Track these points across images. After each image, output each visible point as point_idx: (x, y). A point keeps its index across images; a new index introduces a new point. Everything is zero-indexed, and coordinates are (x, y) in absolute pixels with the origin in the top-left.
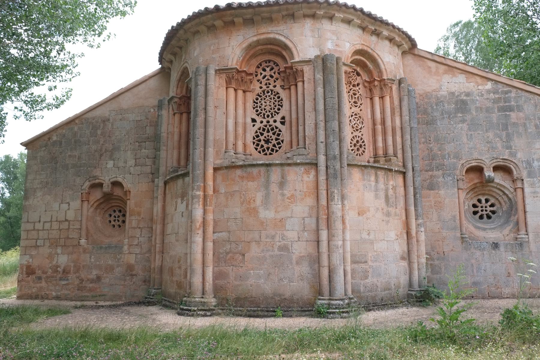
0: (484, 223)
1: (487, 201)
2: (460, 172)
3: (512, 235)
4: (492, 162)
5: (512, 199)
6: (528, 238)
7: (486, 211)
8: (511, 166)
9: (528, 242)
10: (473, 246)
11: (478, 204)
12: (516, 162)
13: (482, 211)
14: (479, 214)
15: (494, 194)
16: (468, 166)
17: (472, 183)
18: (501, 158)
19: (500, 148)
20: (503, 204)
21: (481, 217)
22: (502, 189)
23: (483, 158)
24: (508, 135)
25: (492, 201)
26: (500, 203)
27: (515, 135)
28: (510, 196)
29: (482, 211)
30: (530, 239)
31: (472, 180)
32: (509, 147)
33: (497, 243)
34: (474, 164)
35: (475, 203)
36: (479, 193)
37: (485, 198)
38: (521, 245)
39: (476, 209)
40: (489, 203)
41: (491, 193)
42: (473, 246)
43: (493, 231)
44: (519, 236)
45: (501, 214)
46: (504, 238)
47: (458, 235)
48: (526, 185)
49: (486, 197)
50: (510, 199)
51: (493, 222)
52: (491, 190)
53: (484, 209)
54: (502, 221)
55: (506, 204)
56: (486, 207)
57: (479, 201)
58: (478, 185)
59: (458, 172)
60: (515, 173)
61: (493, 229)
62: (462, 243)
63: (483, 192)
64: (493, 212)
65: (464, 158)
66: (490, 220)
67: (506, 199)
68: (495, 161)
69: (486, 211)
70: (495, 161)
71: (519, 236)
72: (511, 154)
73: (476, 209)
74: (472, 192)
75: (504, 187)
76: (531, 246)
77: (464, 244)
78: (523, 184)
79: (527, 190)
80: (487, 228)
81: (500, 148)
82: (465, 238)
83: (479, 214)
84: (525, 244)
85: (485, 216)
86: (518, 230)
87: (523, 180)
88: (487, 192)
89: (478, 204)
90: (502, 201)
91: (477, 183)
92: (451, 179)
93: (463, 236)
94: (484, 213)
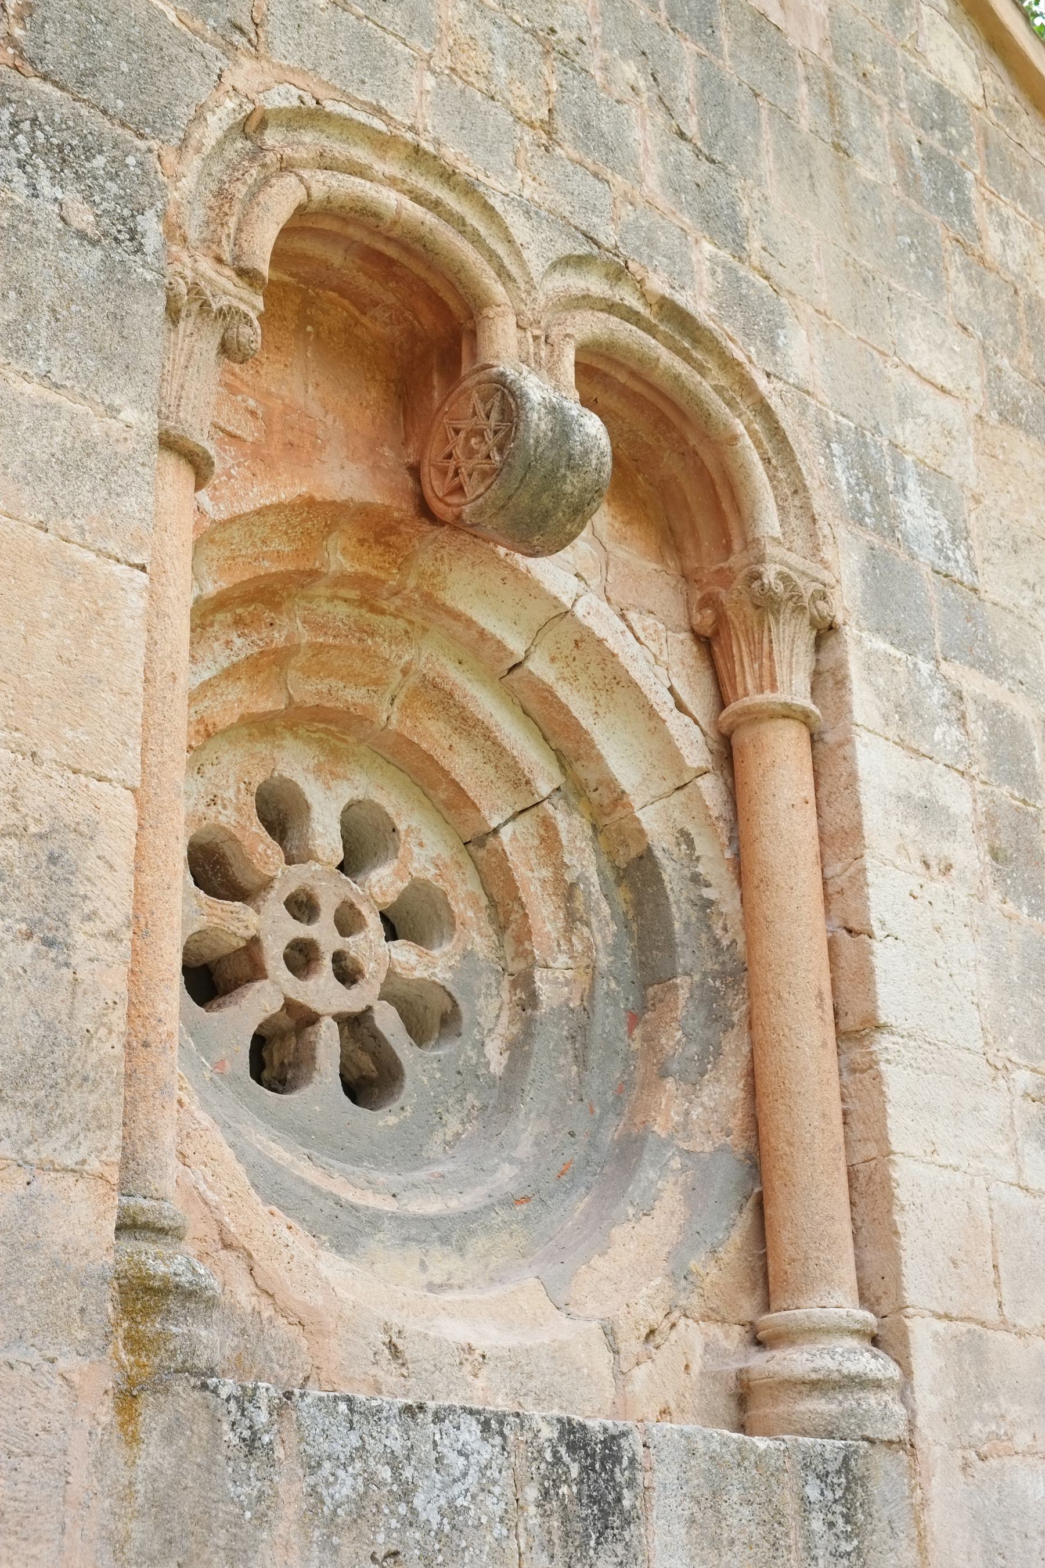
0: (301, 1134)
1: (363, 844)
2: (214, 215)
3: (693, 1335)
4: (578, 282)
5: (671, 873)
6: (905, 1389)
7: (347, 974)
8: (740, 428)
9: (905, 1445)
10: (291, 1488)
11: (262, 851)
12: (774, 402)
13: (301, 957)
14: (257, 1004)
15: (464, 764)
16: (325, 184)
17: (287, 488)
18: (658, 284)
19: (652, 182)
20: (544, 915)
21: (274, 1060)
22: (578, 704)
23: (497, 187)
24: (713, 91)
25: (422, 854)
26: (504, 908)
27: (768, 136)
28: (655, 821)
29: (301, 957)
30: (928, 1401)
31: (286, 441)
32: (725, 225)
33: (612, 1440)
34: (390, 200)
35: (227, 818)
36: (307, 690)
37: (346, 793)
38: (847, 1485)
39: (236, 921)
40: (383, 882)
41: (434, 734)
42: (291, 1488)
43: (443, 1264)
44: (796, 1361)
45: (496, 1061)
46: (620, 1375)
47: (82, 1224)
48: (863, 702)
49: (360, 785)
50: (636, 873)
51: (408, 1152)
52: (440, 698)
53: (323, 932)
54: (525, 1148)
55: (572, 919)
56: (348, 921)
57: (280, 814)
58: (339, 557)
59: (187, 182)
60: (769, 521)
61: (448, 1232)
62: (127, 1399)
63: (353, 695)
64: (433, 1017)
65: (282, 44)
66: (385, 1119)
67: (584, 861)
68: (596, 285)
69: (347, 974)
70: (596, 285)
71: (796, 1361)
72: (734, 296)
73: (236, 921)
74: (242, 646)
75: (613, 681)
76: (936, 1518)
77: (152, 1416)
78: (827, 680)
79: (876, 763)
80: (374, 1220)
81: (652, 182)
82: (192, 1296)
83: (257, 1004)
84: (884, 1473)
85: (328, 1044)
86: (764, 1273)
87: (825, 633)
88: (389, 715)
89: (262, 851)
90: (532, 879)
91: (317, 515)
92: (83, 218)
93: (163, 1262)
94: (322, 992)
